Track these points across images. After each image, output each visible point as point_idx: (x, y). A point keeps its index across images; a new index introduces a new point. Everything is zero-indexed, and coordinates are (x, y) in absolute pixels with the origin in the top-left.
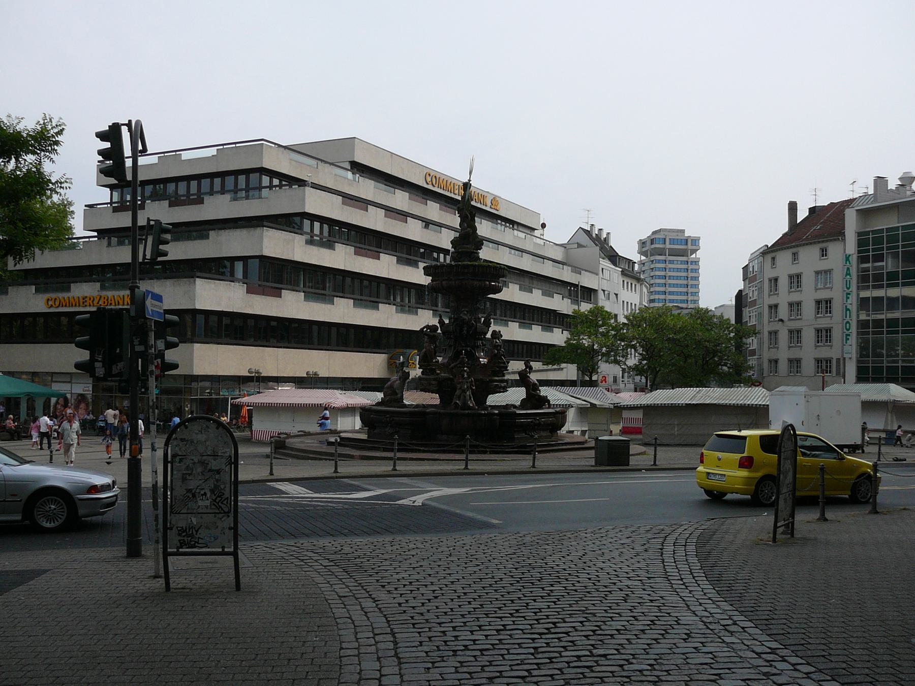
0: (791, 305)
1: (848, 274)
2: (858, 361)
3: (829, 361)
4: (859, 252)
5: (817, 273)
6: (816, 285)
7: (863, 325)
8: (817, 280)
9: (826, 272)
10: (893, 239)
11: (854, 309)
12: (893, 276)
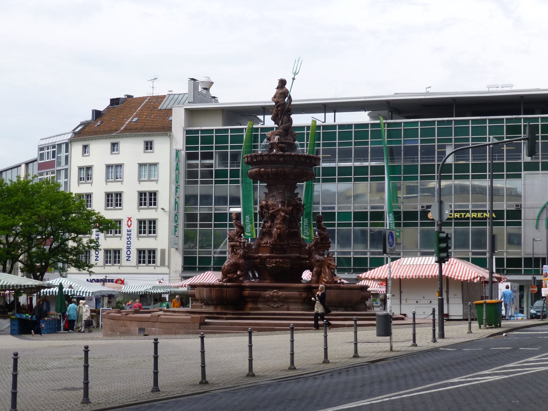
0: (108, 195)
1: (177, 169)
2: (185, 252)
3: (152, 252)
4: (187, 148)
5: (141, 165)
6: (140, 176)
7: (190, 218)
9: (151, 165)
10: (222, 140)
11: (182, 201)
12: (219, 174)
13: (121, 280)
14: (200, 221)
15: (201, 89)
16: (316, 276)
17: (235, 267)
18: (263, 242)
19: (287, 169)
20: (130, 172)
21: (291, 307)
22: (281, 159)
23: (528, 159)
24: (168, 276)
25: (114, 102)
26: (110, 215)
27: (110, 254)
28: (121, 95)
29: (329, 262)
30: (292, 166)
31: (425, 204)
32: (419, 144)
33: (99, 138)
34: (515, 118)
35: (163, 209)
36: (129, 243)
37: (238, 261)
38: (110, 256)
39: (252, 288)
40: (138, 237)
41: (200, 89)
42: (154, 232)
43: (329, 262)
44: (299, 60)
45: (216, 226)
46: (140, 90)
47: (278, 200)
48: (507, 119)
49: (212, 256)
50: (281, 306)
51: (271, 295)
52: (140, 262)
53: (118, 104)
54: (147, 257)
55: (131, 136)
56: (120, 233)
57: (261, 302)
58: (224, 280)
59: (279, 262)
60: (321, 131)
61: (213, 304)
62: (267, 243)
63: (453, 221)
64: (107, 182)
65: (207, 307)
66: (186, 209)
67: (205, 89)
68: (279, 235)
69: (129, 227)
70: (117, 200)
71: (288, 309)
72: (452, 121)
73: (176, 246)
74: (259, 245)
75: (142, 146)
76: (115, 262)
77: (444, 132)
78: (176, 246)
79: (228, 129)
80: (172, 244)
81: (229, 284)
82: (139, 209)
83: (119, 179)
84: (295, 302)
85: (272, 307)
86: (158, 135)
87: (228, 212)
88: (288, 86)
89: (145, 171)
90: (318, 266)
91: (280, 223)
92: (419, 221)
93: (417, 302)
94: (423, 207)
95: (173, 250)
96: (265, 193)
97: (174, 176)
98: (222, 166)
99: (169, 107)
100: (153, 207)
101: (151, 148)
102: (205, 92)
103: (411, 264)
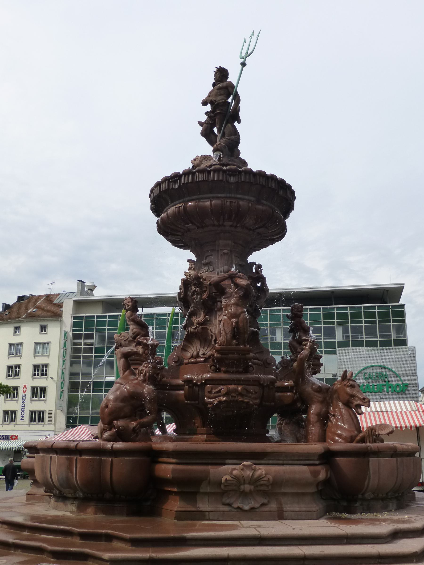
1: (65, 346)
2: (68, 413)
3: (42, 413)
4: (74, 331)
5: (37, 344)
6: (35, 352)
7: (74, 385)
8: (35, 349)
9: (45, 343)
10: (101, 324)
13: (15, 436)
14: (81, 388)
15: (85, 288)
16: (318, 425)
17: (132, 405)
18: (189, 355)
19: (244, 202)
20: (28, 349)
21: (290, 507)
22: (232, 180)
23: (341, 339)
24: (53, 433)
25: (21, 298)
26: (11, 383)
27: (8, 414)
28: (27, 294)
29: (348, 390)
30: (253, 199)
33: (5, 324)
34: (329, 308)
35: (52, 378)
36: (23, 405)
37: (139, 389)
38: (8, 416)
39: (181, 456)
40: (31, 401)
41: (86, 290)
42: (44, 397)
43: (348, 390)
44: (252, 35)
45: (94, 391)
46: (40, 290)
47: (221, 269)
48: (323, 308)
49: (90, 416)
50: (263, 505)
51: (236, 478)
52: (31, 421)
53: (23, 300)
54: (37, 416)
55: (30, 322)
56: (16, 397)
58: (107, 434)
59: (236, 390)
61: (75, 499)
62: (198, 356)
64: (9, 357)
65: (61, 505)
66: (70, 378)
67: (89, 289)
68: (237, 333)
69: (24, 392)
70: (16, 371)
71: (280, 516)
72: (280, 310)
73: (61, 408)
74: (179, 362)
75: (38, 329)
76: (12, 421)
78: (61, 408)
79: (106, 316)
80: (58, 406)
81: (119, 445)
82: (33, 378)
83: (19, 355)
84: (297, 495)
85: (238, 508)
86: (51, 321)
87: (104, 380)
88: (232, 78)
89: (40, 349)
90: (322, 402)
91: (236, 304)
95: (59, 411)
96: (189, 261)
97: (62, 351)
98: (100, 344)
99: (62, 301)
100: (44, 376)
101: (45, 331)
102: (89, 291)
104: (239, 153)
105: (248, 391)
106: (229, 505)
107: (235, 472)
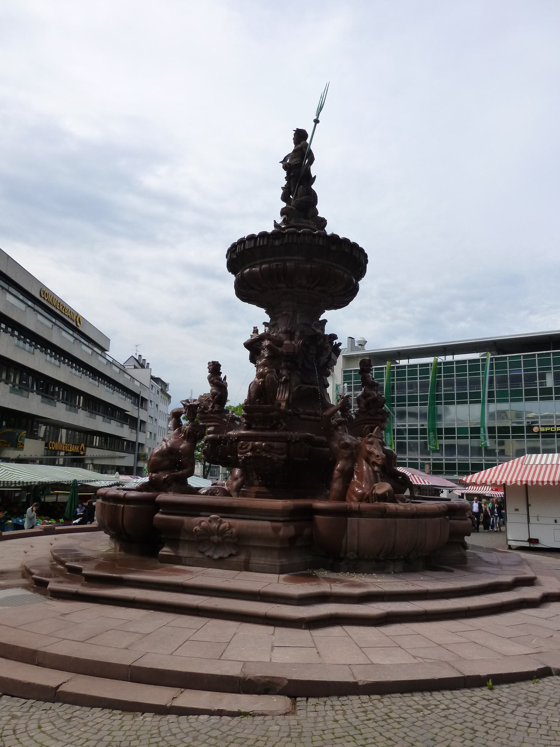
21: (257, 560)
22: (277, 243)
29: (368, 447)
31: (530, 421)
32: (523, 373)
41: (356, 345)
43: (368, 447)
50: (231, 555)
57: (187, 541)
59: (260, 447)
60: (442, 366)
63: (556, 434)
71: (246, 567)
77: (544, 362)
84: (262, 548)
85: (209, 556)
90: (347, 458)
92: (525, 434)
93: (556, 521)
94: (528, 422)
103: (543, 463)
104: (317, 212)
105: (272, 447)
106: (202, 553)
107: (203, 524)
